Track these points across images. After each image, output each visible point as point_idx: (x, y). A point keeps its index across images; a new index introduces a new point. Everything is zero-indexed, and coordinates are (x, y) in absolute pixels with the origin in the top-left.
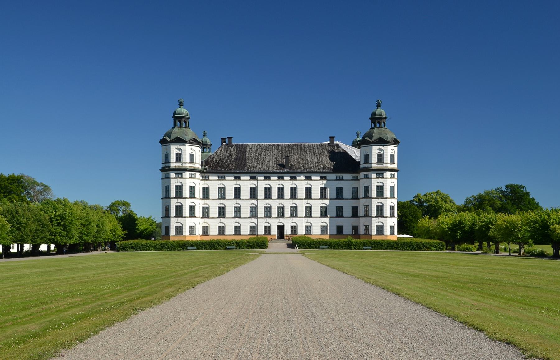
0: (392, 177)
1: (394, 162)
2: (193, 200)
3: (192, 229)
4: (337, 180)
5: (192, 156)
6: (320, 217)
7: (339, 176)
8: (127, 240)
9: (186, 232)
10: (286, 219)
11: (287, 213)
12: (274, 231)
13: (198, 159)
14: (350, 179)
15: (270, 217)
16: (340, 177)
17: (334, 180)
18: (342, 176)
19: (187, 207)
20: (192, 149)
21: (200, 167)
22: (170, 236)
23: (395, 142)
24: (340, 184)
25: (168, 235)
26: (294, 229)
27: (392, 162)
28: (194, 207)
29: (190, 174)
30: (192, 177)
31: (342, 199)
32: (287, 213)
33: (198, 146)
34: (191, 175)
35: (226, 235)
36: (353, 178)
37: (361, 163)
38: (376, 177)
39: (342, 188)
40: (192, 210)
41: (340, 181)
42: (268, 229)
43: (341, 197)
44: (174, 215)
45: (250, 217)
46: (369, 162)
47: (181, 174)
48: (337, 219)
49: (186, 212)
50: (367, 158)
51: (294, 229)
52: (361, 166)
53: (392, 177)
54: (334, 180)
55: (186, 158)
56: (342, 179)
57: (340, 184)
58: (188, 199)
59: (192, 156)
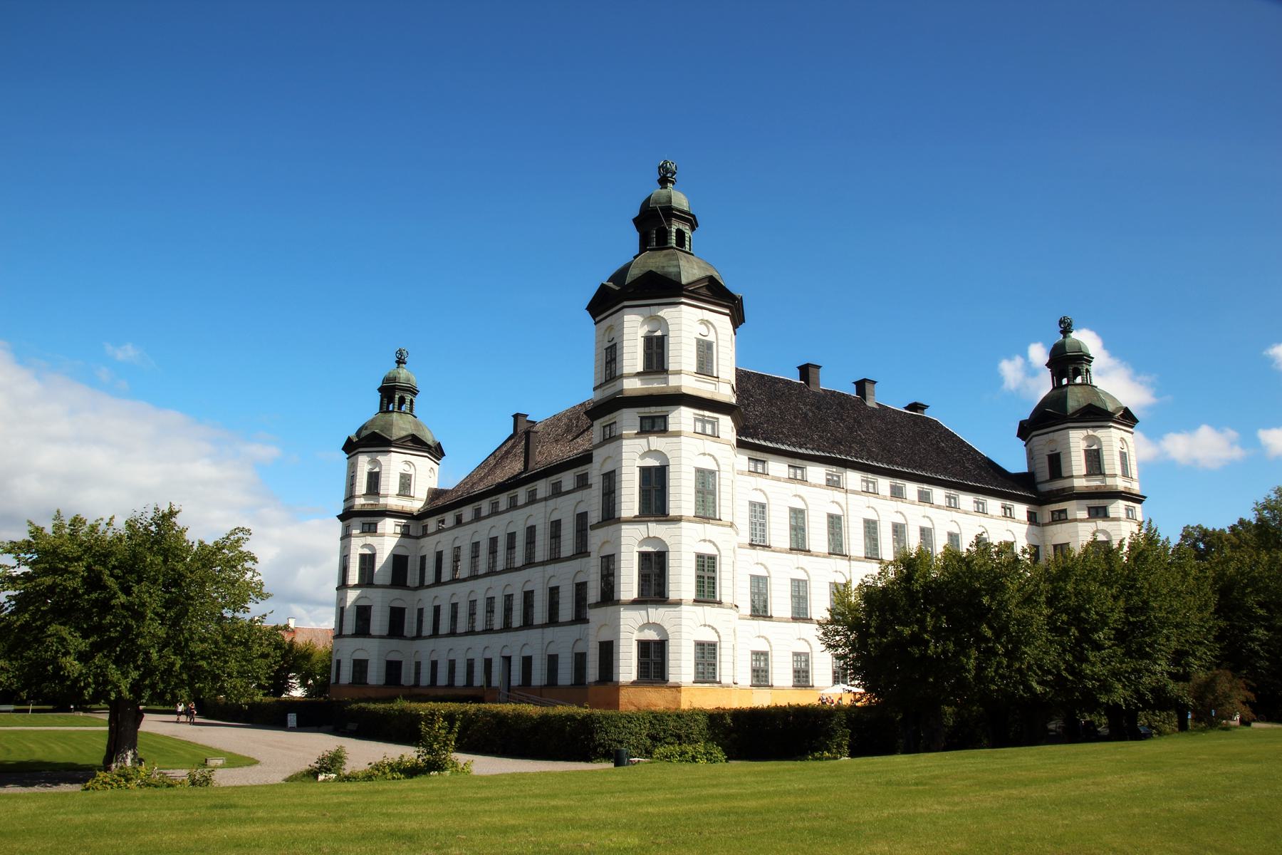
2: (709, 530)
3: (707, 653)
5: (705, 351)
8: (460, 703)
9: (682, 667)
13: (726, 365)
19: (684, 556)
20: (705, 322)
21: (733, 400)
22: (617, 687)
25: (611, 680)
28: (712, 558)
29: (696, 420)
30: (704, 433)
33: (727, 311)
34: (699, 425)
40: (706, 574)
44: (635, 595)
47: (665, 418)
49: (682, 581)
55: (682, 357)
58: (689, 521)
59: (705, 351)
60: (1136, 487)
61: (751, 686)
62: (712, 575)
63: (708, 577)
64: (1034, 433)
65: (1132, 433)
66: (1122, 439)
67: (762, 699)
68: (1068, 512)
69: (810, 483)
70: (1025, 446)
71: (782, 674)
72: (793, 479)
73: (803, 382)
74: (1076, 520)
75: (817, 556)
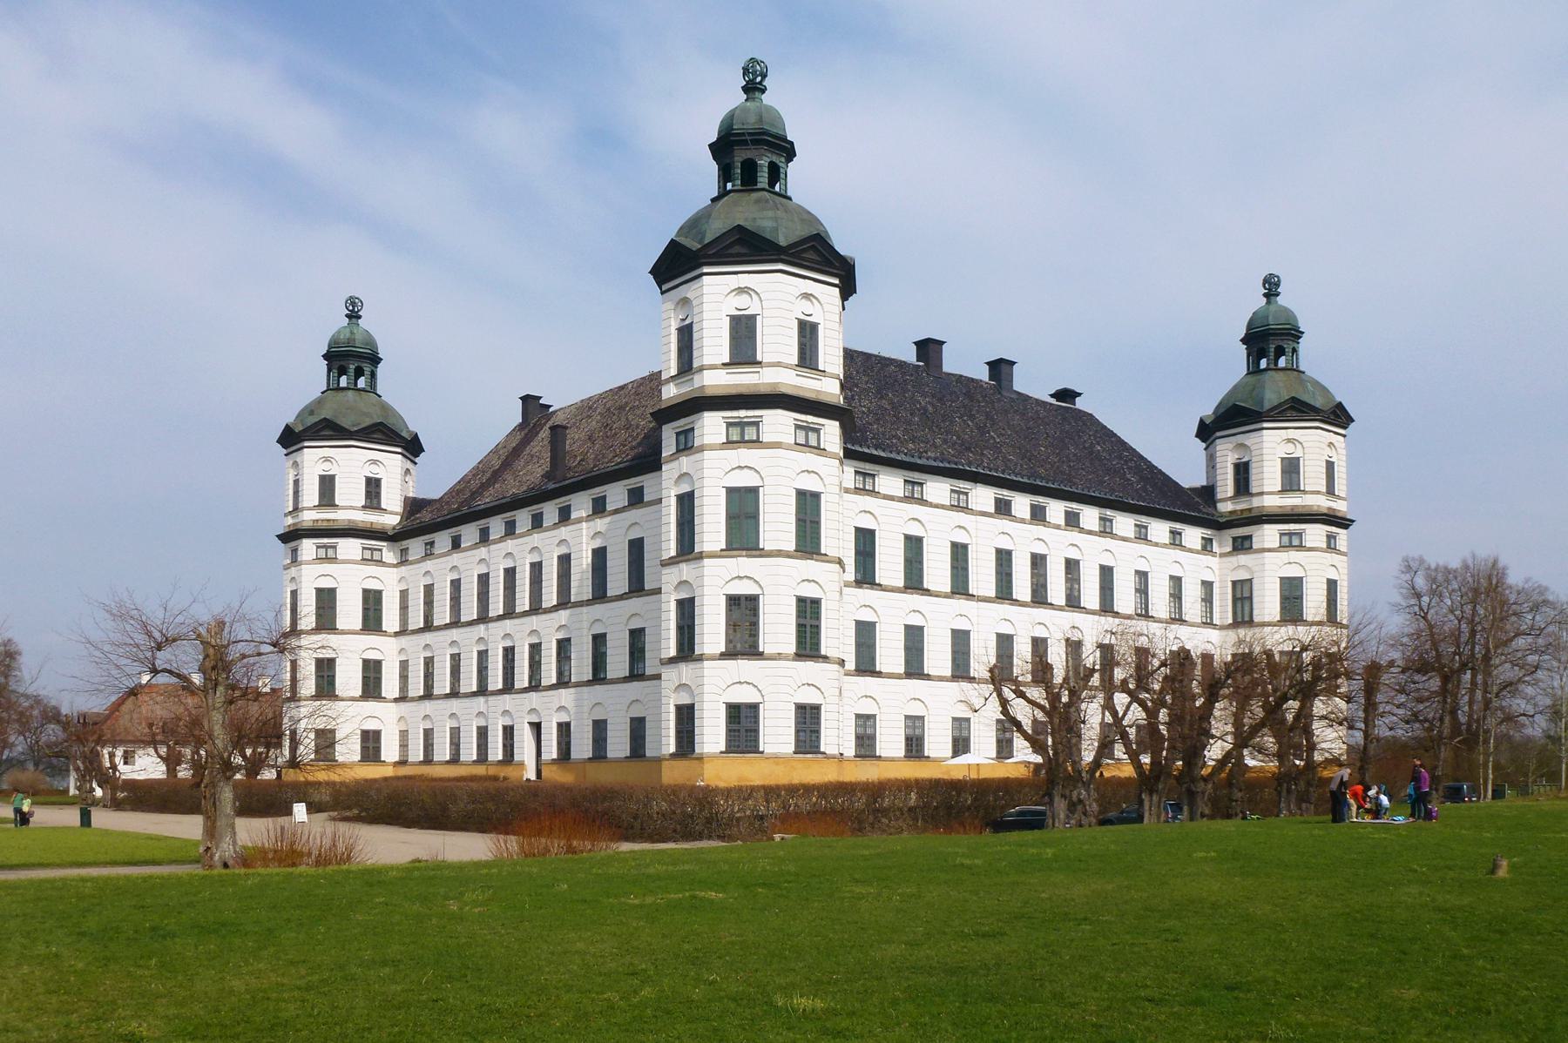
0: (1333, 546)
23: (1338, 417)
27: (1330, 491)
38: (1278, 545)
46: (1254, 490)
50: (1242, 472)
53: (1331, 546)
60: (1341, 507)
61: (855, 757)
62: (814, 623)
63: (811, 626)
64: (1218, 434)
65: (1344, 436)
66: (1331, 444)
67: (868, 773)
68: (1254, 539)
69: (931, 503)
70: (1205, 449)
71: (891, 743)
72: (909, 499)
73: (921, 364)
74: (1264, 550)
75: (937, 596)
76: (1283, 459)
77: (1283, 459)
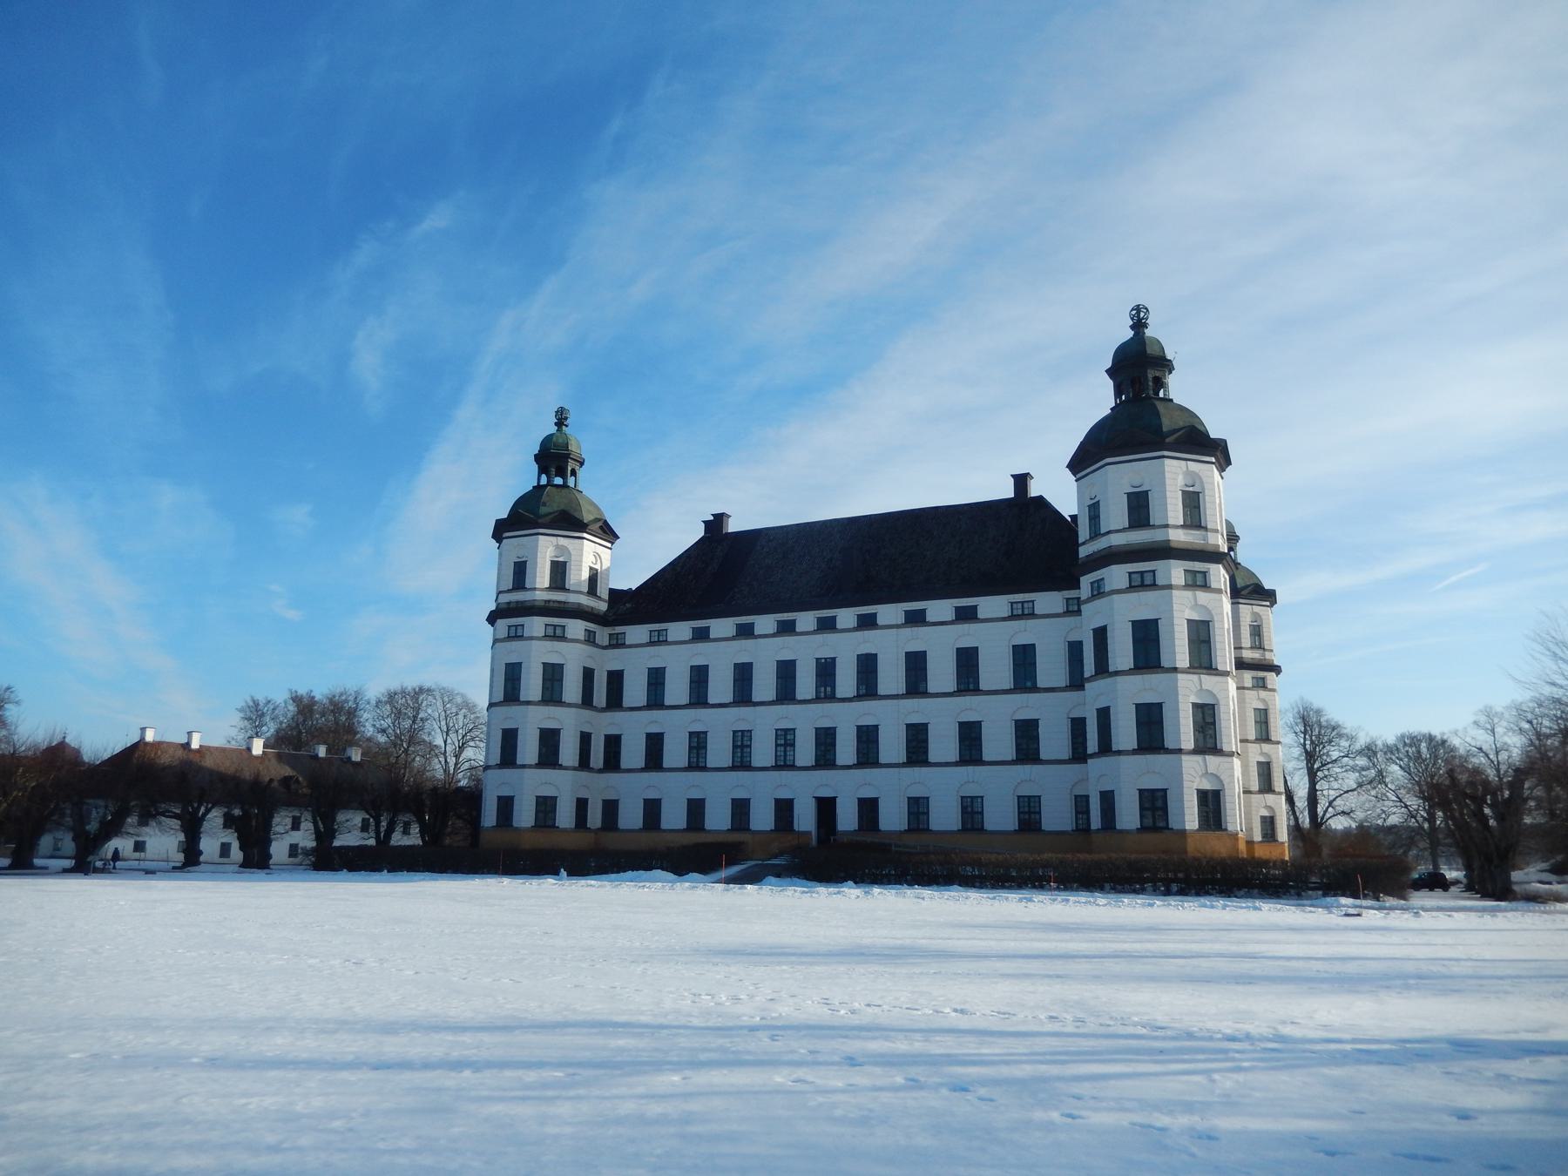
1: (1203, 525)
4: (1013, 617)
6: (956, 764)
7: (1023, 603)
10: (841, 772)
11: (846, 750)
12: (805, 819)
14: (1060, 609)
15: (792, 767)
16: (1026, 605)
17: (1004, 619)
18: (1033, 601)
24: (1024, 633)
26: (869, 807)
31: (1035, 689)
32: (846, 750)
35: (665, 831)
36: (1071, 609)
37: (1081, 540)
39: (1034, 645)
41: (1022, 622)
42: (784, 809)
43: (1029, 684)
45: (733, 768)
48: (1019, 768)
51: (869, 807)
52: (1084, 552)
54: (1004, 619)
56: (1032, 615)
57: (1024, 633)
76: (1129, 495)
77: (1129, 495)
